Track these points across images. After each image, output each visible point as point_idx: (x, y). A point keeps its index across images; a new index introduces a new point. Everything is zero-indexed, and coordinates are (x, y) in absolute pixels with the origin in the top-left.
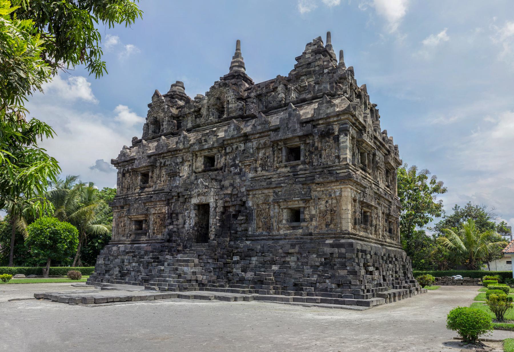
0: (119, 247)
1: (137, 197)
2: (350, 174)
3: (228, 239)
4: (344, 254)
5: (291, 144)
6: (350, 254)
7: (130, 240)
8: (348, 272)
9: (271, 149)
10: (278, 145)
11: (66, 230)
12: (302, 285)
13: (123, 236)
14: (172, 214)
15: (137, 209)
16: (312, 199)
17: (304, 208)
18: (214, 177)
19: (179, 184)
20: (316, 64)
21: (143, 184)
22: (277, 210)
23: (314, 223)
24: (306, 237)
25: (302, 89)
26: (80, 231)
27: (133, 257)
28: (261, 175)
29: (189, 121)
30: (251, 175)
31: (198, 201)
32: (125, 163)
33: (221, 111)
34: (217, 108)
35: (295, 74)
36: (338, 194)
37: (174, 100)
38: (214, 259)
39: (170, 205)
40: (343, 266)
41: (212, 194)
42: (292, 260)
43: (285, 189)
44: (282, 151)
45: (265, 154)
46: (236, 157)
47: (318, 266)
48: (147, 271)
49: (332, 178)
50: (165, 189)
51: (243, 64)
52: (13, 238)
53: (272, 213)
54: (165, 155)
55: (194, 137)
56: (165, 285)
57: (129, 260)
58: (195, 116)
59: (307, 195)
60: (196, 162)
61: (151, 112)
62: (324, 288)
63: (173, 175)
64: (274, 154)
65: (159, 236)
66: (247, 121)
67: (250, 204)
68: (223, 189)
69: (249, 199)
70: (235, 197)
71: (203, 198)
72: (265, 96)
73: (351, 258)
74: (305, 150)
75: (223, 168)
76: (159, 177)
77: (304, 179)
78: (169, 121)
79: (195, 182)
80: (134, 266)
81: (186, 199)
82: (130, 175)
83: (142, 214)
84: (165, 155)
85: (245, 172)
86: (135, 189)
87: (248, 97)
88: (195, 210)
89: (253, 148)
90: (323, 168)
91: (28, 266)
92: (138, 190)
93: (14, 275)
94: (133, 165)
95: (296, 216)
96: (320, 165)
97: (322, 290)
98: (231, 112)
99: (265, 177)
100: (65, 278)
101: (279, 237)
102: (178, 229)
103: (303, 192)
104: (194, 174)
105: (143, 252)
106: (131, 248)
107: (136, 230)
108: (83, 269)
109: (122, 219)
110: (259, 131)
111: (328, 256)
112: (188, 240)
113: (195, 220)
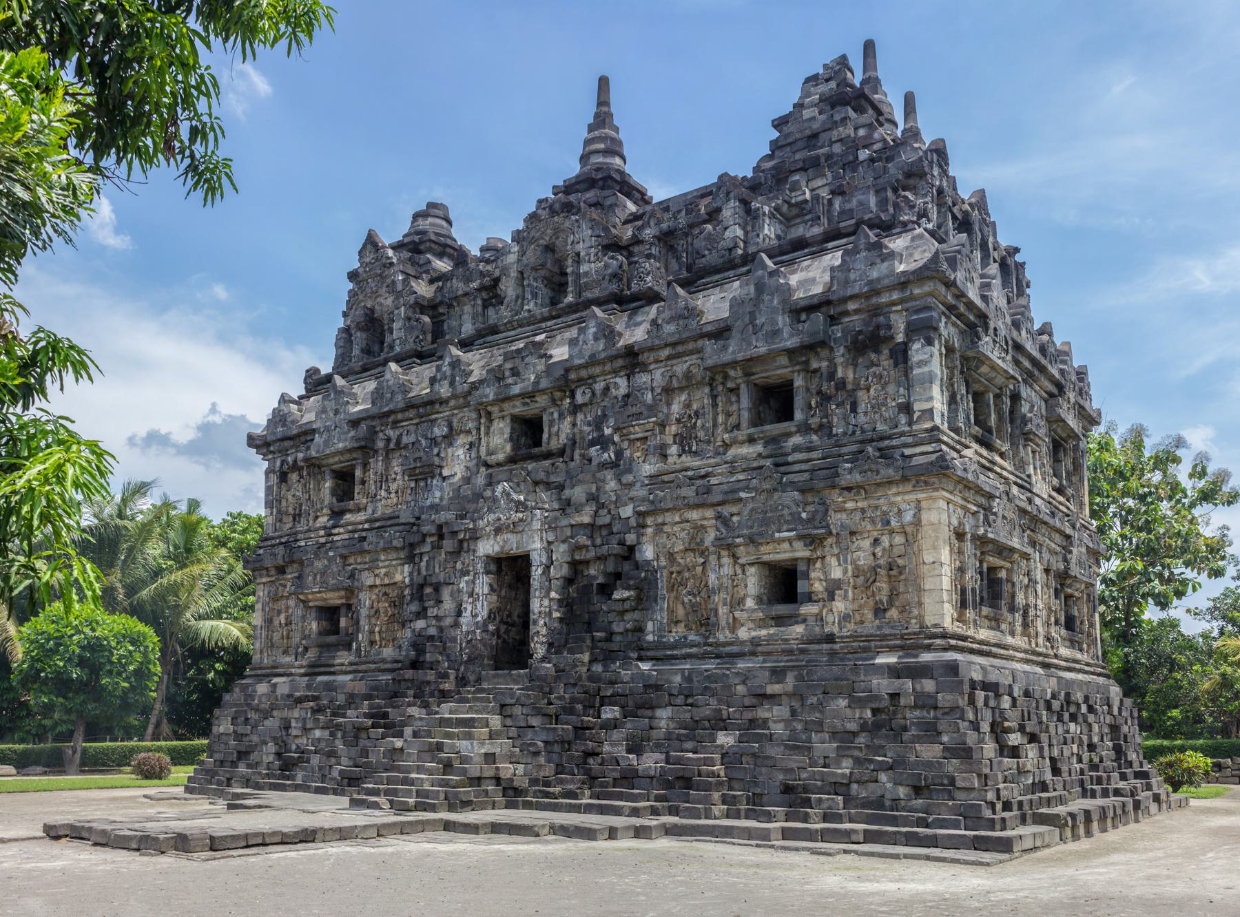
0: (275, 685)
1: (323, 540)
2: (943, 458)
4: (932, 696)
6: (949, 697)
8: (946, 749)
9: (707, 390)
10: (726, 377)
12: (806, 789)
13: (285, 652)
14: (421, 587)
15: (323, 574)
16: (830, 533)
17: (810, 561)
19: (441, 499)
21: (339, 501)
22: (727, 570)
23: (839, 606)
24: (817, 647)
26: (164, 640)
28: (678, 467)
30: (648, 469)
31: (497, 549)
32: (287, 444)
33: (557, 285)
36: (908, 517)
39: (417, 559)
40: (931, 732)
41: (537, 525)
42: (775, 716)
43: (750, 506)
44: (738, 396)
45: (688, 405)
46: (604, 415)
50: (402, 514)
53: (712, 578)
54: (400, 416)
55: (482, 363)
57: (304, 720)
59: (817, 523)
60: (487, 434)
63: (424, 473)
64: (715, 405)
65: (388, 652)
68: (569, 511)
70: (604, 533)
72: (686, 235)
74: (808, 390)
75: (568, 451)
76: (384, 479)
77: (806, 476)
79: (488, 493)
80: (319, 740)
81: (461, 541)
82: (301, 477)
83: (338, 589)
84: (400, 416)
85: (632, 460)
86: (317, 517)
87: (636, 241)
88: (488, 572)
89: (653, 390)
90: (862, 442)
92: (325, 519)
94: (308, 448)
95: (785, 585)
96: (854, 433)
98: (587, 287)
99: (690, 473)
101: (735, 649)
102: (441, 629)
103: (804, 515)
104: (483, 469)
106: (309, 687)
107: (320, 633)
109: (281, 604)
110: (670, 340)
112: (471, 660)
113: (490, 603)
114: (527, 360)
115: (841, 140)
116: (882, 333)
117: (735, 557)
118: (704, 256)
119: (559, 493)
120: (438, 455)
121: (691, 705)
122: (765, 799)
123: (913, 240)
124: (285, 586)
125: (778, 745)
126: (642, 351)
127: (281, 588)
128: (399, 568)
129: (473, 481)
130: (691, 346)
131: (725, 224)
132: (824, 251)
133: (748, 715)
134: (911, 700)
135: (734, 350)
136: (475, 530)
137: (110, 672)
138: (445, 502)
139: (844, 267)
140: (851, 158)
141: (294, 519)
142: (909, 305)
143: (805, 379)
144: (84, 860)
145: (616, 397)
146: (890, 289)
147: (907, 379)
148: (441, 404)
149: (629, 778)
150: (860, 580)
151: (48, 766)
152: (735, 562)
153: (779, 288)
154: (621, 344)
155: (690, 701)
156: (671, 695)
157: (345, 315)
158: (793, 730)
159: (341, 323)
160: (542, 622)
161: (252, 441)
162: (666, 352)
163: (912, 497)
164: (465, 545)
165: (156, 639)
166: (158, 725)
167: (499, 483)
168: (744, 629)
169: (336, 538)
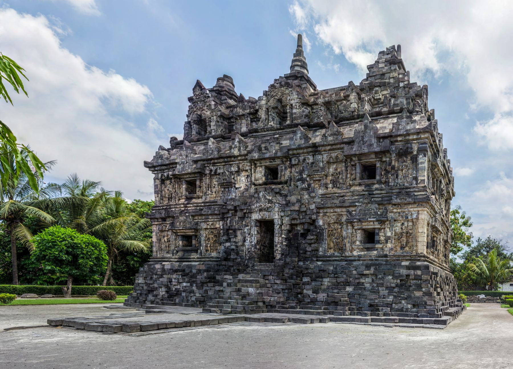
1: (183, 209)
2: (428, 196)
3: (297, 259)
4: (420, 276)
5: (364, 160)
6: (425, 276)
7: (177, 257)
8: (424, 293)
9: (344, 164)
10: (351, 160)
11: (88, 243)
12: (377, 306)
13: (168, 253)
14: (228, 230)
15: (184, 222)
16: (388, 220)
17: (380, 229)
18: (278, 191)
19: (236, 196)
20: (391, 75)
21: (189, 194)
22: (350, 231)
23: (389, 245)
24: (381, 259)
25: (376, 102)
26: (108, 246)
27: (182, 276)
28: (332, 192)
29: (242, 125)
30: (321, 192)
31: (260, 217)
32: (163, 167)
33: (282, 116)
34: (277, 113)
35: (368, 84)
36: (414, 216)
37: (223, 98)
38: (282, 279)
39: (225, 219)
40: (419, 287)
41: (276, 209)
42: (367, 282)
43: (360, 208)
44: (356, 168)
45: (336, 170)
46: (303, 170)
47: (394, 288)
48: (201, 291)
49: (410, 200)
50: (218, 201)
51: (306, 65)
52: (14, 250)
53: (344, 233)
54: (216, 161)
55: (252, 143)
56: (228, 307)
57: (178, 279)
58: (251, 119)
59: (383, 216)
60: (255, 172)
61: (192, 108)
62: (400, 308)
63: (228, 185)
64: (347, 170)
65: (214, 254)
66: (315, 131)
67: (321, 223)
68: (289, 205)
69: (319, 218)
70: (303, 214)
71: (266, 213)
72: (335, 104)
73: (426, 280)
74: (381, 168)
76: (209, 187)
77: (380, 199)
78: (218, 122)
79: (256, 195)
80: (185, 287)
81: (245, 213)
82: (171, 182)
83: (191, 229)
84: (216, 161)
85: (314, 188)
86: (179, 200)
88: (256, 226)
89: (323, 162)
90: (400, 189)
91: (41, 284)
92: (184, 200)
93: (19, 294)
94: (174, 170)
95: (370, 237)
96: (397, 186)
97: (397, 310)
99: (337, 195)
100: (94, 298)
101: (352, 258)
102: (237, 247)
103: (379, 213)
104: (253, 186)
105: (194, 271)
106: (179, 266)
107: (183, 246)
108: (117, 289)
109: (165, 233)
111: (404, 278)
112: (250, 259)
113: (257, 238)
114: (271, 144)
115: (393, 78)
116: (409, 150)
117: (353, 226)
118: (342, 113)
119: (285, 198)
120: (234, 178)
121: (337, 277)
122: (363, 309)
123: (421, 117)
124: (166, 226)
125: (368, 291)
126: (319, 146)
127: (164, 227)
128: (218, 222)
129: (249, 190)
130: (338, 146)
131: (351, 101)
132: (388, 118)
133: (357, 281)
134: (413, 277)
135: (355, 149)
136: (251, 209)
137: (83, 258)
138: (237, 198)
139: (398, 124)
140: (397, 85)
141: (169, 200)
142: (419, 141)
143: (380, 164)
144: (71, 337)
145: (308, 163)
146: (413, 134)
147: (417, 168)
148: (234, 158)
149: (314, 301)
150: (397, 237)
151: (55, 294)
152: (353, 228)
153: (373, 128)
154: (310, 142)
155: (336, 276)
156: (329, 274)
157: (188, 116)
158: (373, 286)
159: (186, 120)
160: (279, 246)
161: (146, 164)
162: (328, 148)
163: (416, 209)
164: (247, 215)
165: (105, 246)
166: (109, 280)
167: (260, 192)
168: (355, 252)
169: (189, 208)
